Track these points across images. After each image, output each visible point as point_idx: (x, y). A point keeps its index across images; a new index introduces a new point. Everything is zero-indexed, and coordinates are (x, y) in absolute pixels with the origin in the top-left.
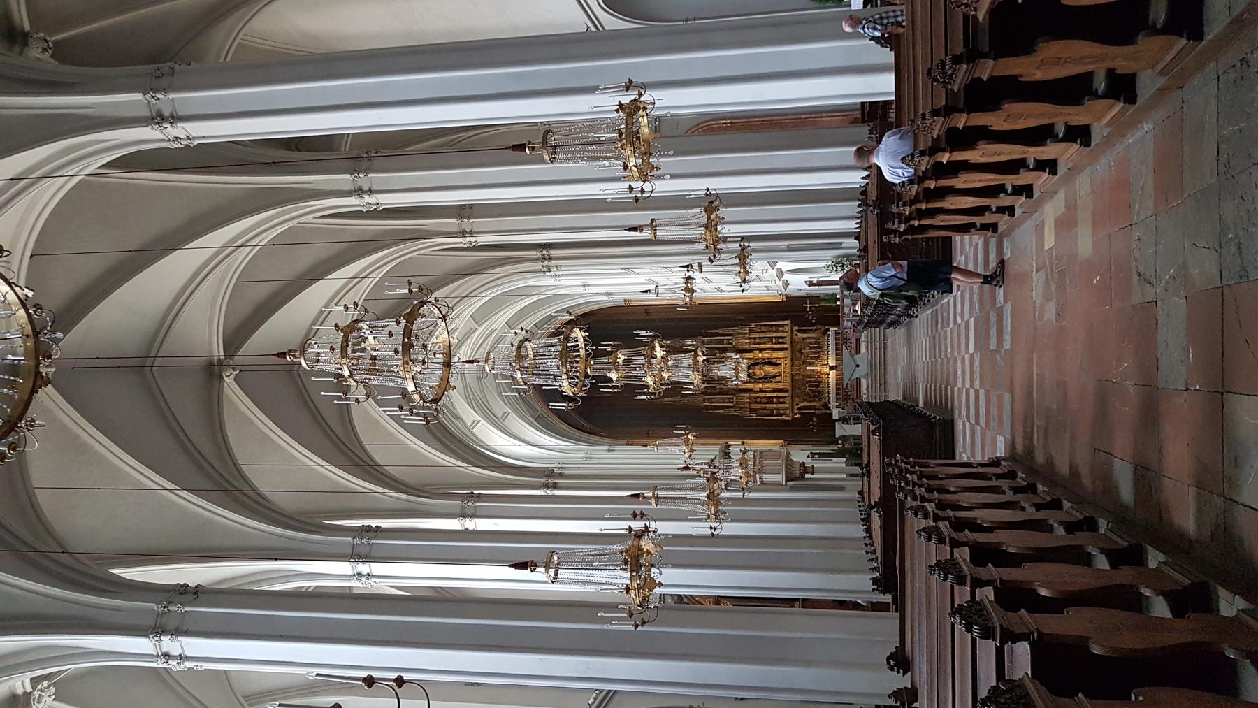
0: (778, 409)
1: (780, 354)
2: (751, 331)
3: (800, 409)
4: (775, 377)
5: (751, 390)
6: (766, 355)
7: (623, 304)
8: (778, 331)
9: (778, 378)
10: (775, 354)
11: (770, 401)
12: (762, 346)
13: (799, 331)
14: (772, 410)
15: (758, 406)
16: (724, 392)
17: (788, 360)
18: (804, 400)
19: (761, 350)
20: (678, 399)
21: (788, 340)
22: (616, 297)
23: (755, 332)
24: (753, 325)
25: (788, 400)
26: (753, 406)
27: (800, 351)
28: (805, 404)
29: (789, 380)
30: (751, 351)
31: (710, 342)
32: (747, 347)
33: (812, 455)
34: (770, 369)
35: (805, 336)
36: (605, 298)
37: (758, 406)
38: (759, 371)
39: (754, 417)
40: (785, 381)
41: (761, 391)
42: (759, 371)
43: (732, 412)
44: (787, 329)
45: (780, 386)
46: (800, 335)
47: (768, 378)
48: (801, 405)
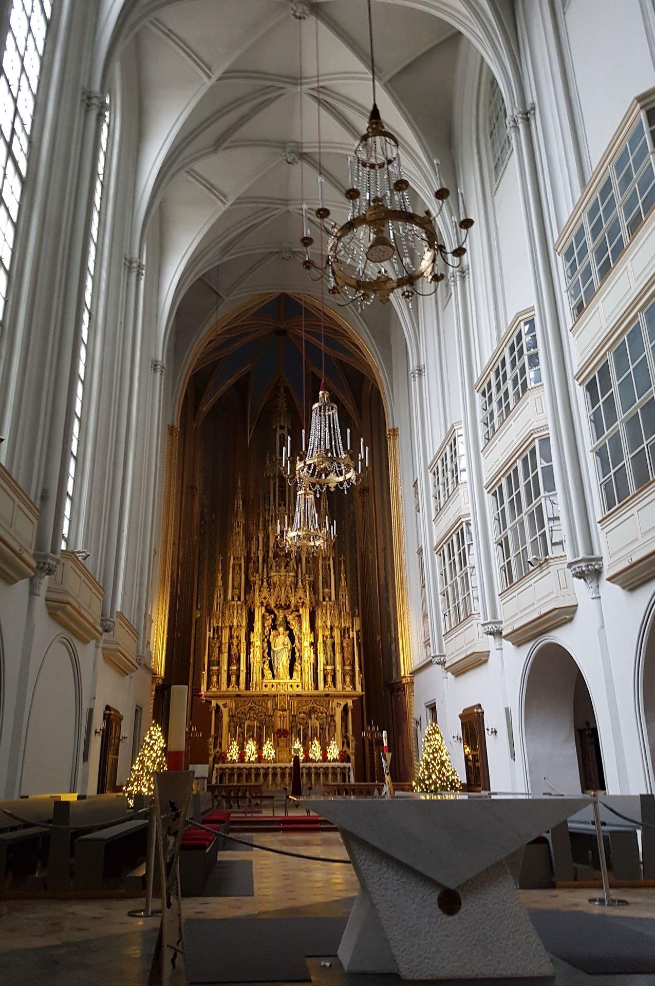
0: (219, 673)
1: (308, 677)
2: (344, 632)
3: (217, 706)
4: (271, 668)
5: (250, 628)
6: (307, 654)
7: (389, 426)
8: (344, 676)
9: (268, 673)
10: (308, 667)
11: (233, 659)
12: (320, 646)
13: (346, 706)
14: (218, 664)
15: (225, 639)
16: (249, 586)
17: (299, 690)
18: (231, 717)
19: (314, 644)
20: (241, 520)
21: (331, 690)
22: (414, 384)
23: (342, 637)
24: (353, 634)
25: (233, 690)
26: (226, 634)
27: (312, 711)
28: (226, 719)
29: (266, 691)
30: (313, 628)
31: (326, 569)
32: (319, 623)
33: (112, 717)
34: (283, 661)
35: (338, 719)
36: (413, 366)
37: (225, 639)
38: (281, 642)
39: (209, 634)
40: (265, 684)
41: (249, 644)
42: (281, 642)
43: (217, 600)
44: (349, 689)
45: (256, 676)
46: (339, 712)
47: (269, 653)
48: (225, 712)
